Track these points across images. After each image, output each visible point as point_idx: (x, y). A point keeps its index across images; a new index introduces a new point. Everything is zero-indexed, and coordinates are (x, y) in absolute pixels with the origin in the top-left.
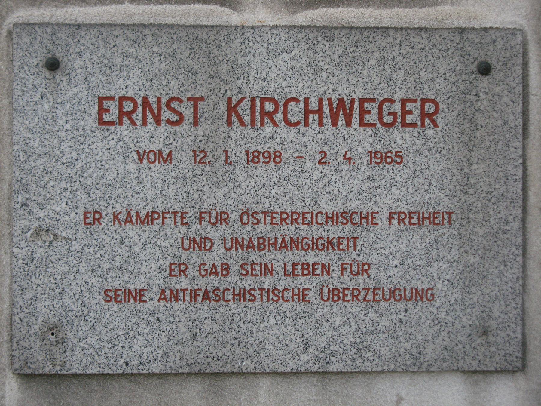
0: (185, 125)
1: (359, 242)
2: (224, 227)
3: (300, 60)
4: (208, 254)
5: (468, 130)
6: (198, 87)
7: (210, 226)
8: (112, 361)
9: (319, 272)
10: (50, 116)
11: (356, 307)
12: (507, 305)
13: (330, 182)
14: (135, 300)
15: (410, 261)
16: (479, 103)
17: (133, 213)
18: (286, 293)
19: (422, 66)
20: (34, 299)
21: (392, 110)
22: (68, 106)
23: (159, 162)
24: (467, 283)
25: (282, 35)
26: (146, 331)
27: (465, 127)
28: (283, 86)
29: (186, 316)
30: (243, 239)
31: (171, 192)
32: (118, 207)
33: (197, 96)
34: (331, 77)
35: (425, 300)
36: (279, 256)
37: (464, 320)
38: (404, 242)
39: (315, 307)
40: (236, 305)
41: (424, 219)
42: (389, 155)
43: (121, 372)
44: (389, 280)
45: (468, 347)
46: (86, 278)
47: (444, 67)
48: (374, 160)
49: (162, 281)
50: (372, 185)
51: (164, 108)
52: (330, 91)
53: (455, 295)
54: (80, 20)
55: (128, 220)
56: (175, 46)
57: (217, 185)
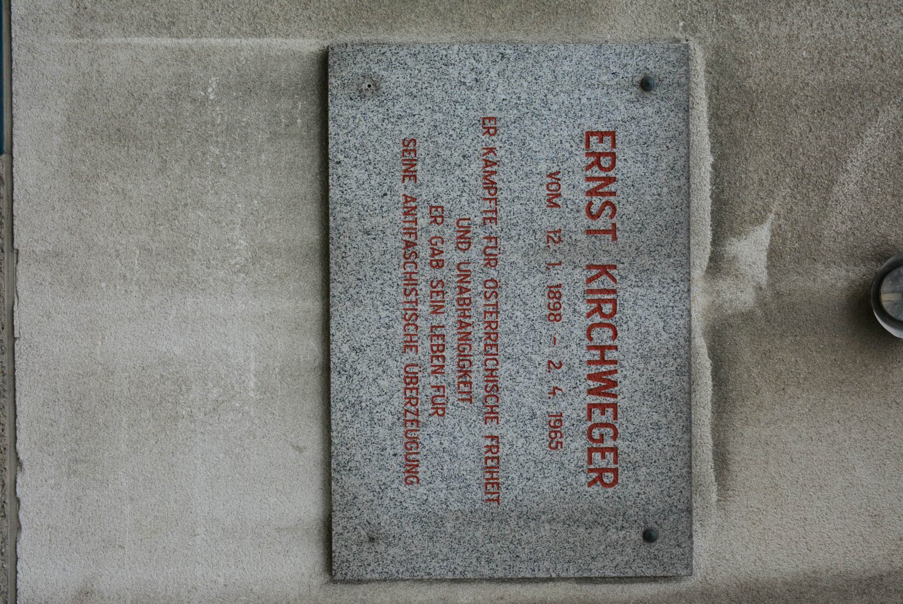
0: (586, 221)
1: (466, 405)
2: (482, 262)
3: (657, 340)
4: (454, 246)
5: (586, 519)
6: (626, 235)
7: (482, 248)
8: (341, 147)
9: (435, 362)
10: (594, 82)
11: (398, 401)
12: (401, 563)
13: (529, 372)
14: (405, 171)
15: (447, 458)
16: (614, 530)
17: (495, 168)
18: (412, 328)
19: (652, 469)
20: (405, 66)
21: (605, 437)
22: (605, 100)
23: (548, 195)
24: (424, 519)
25: (682, 322)
26: (373, 182)
27: (588, 515)
28: (629, 323)
29: (389, 224)
30: (469, 282)
31: (517, 207)
32: (500, 153)
33: (617, 233)
34: (639, 372)
35: (407, 475)
36: (452, 320)
37: (385, 517)
38: (467, 452)
39: (398, 358)
40: (400, 275)
41: (492, 473)
42: (559, 435)
43: (330, 157)
44: (427, 437)
45: (357, 521)
46: (428, 119)
47: (652, 493)
48: (553, 419)
49: (425, 198)
50: (527, 418)
51: (604, 199)
52: (625, 373)
53: (412, 507)
54: (693, 112)
55: (488, 163)
56: (668, 210)
57: (525, 255)
